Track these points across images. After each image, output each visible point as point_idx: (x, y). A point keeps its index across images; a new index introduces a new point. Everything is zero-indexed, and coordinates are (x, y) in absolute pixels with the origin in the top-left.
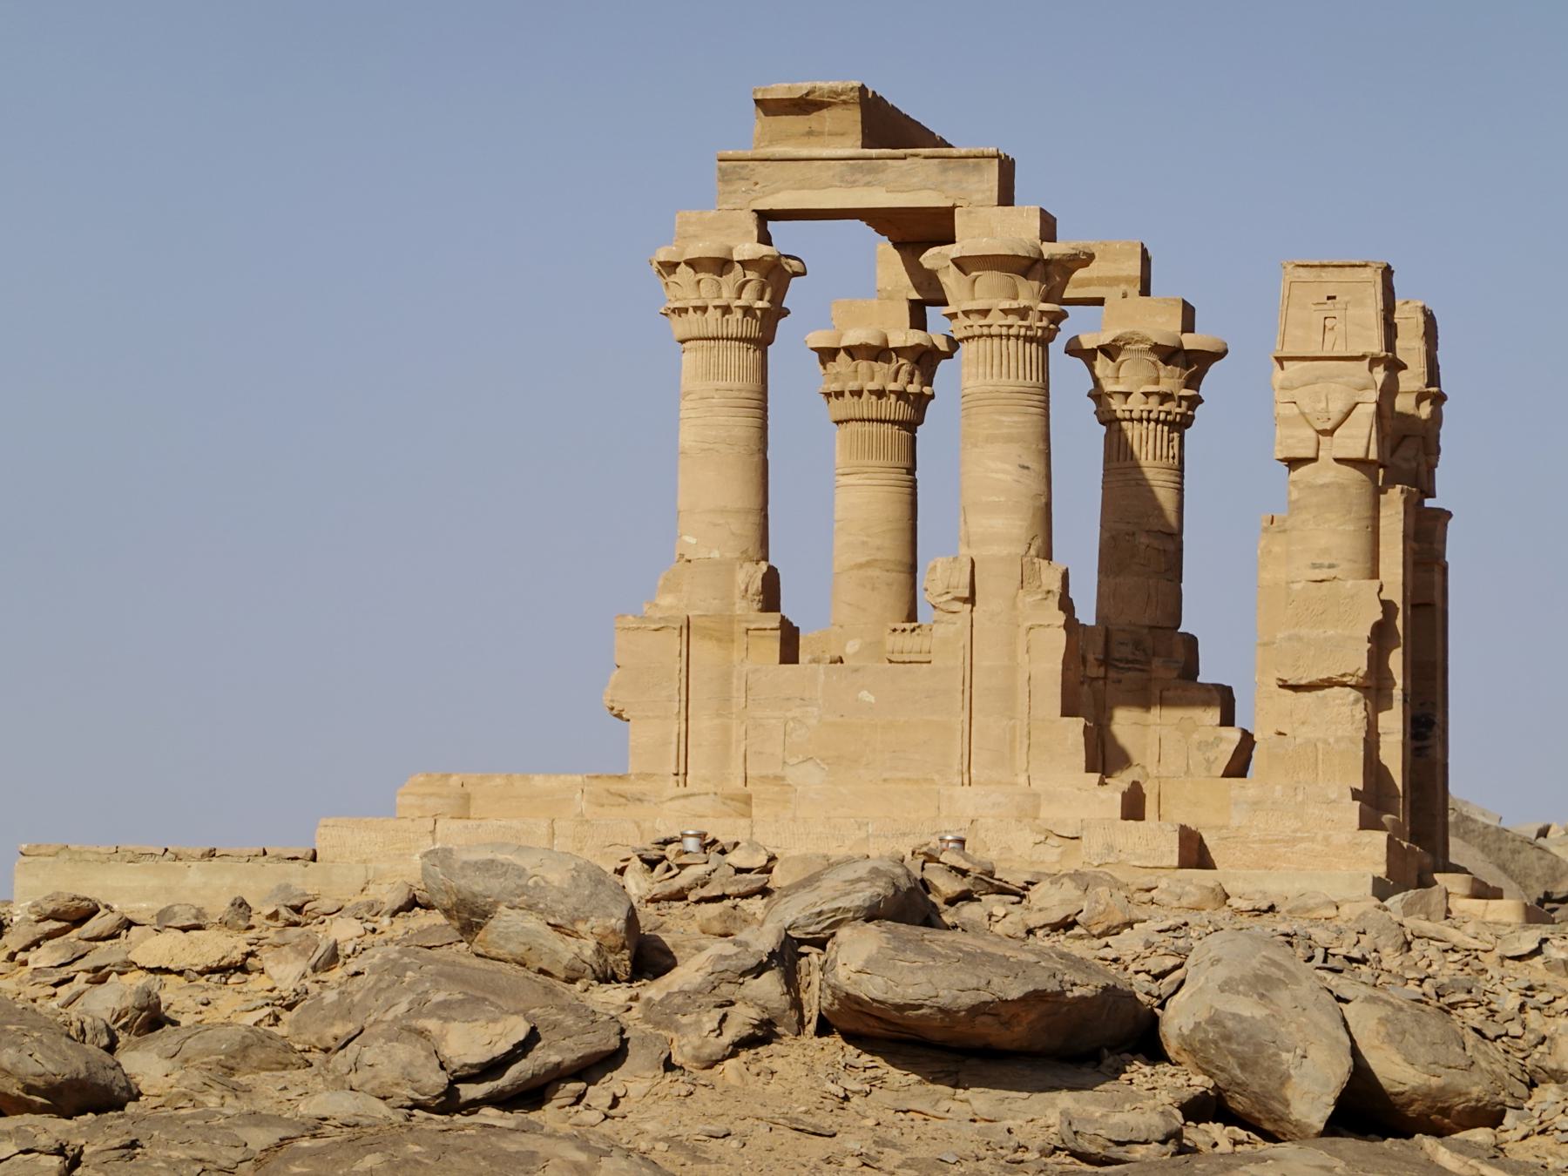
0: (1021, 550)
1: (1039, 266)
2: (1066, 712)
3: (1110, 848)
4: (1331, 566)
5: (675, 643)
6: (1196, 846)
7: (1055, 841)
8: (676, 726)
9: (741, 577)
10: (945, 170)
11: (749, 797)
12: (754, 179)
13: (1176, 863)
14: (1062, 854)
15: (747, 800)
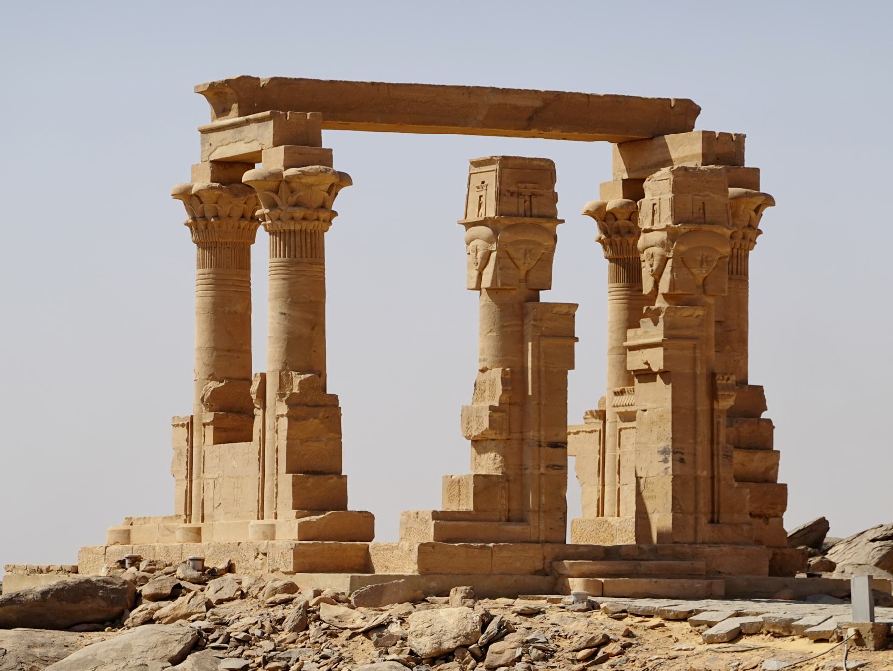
0: (279, 367)
1: (283, 185)
2: (287, 473)
3: (274, 559)
4: (484, 360)
5: (183, 432)
6: (362, 553)
7: (261, 556)
8: (184, 484)
9: (203, 392)
10: (259, 127)
11: (200, 529)
12: (211, 142)
13: (291, 569)
14: (262, 564)
15: (199, 531)
